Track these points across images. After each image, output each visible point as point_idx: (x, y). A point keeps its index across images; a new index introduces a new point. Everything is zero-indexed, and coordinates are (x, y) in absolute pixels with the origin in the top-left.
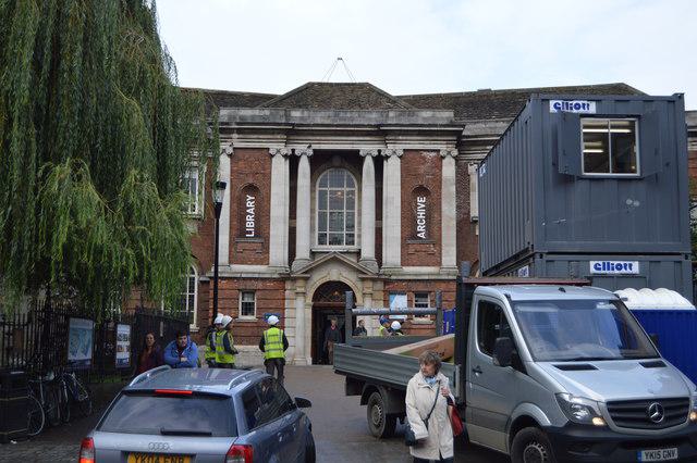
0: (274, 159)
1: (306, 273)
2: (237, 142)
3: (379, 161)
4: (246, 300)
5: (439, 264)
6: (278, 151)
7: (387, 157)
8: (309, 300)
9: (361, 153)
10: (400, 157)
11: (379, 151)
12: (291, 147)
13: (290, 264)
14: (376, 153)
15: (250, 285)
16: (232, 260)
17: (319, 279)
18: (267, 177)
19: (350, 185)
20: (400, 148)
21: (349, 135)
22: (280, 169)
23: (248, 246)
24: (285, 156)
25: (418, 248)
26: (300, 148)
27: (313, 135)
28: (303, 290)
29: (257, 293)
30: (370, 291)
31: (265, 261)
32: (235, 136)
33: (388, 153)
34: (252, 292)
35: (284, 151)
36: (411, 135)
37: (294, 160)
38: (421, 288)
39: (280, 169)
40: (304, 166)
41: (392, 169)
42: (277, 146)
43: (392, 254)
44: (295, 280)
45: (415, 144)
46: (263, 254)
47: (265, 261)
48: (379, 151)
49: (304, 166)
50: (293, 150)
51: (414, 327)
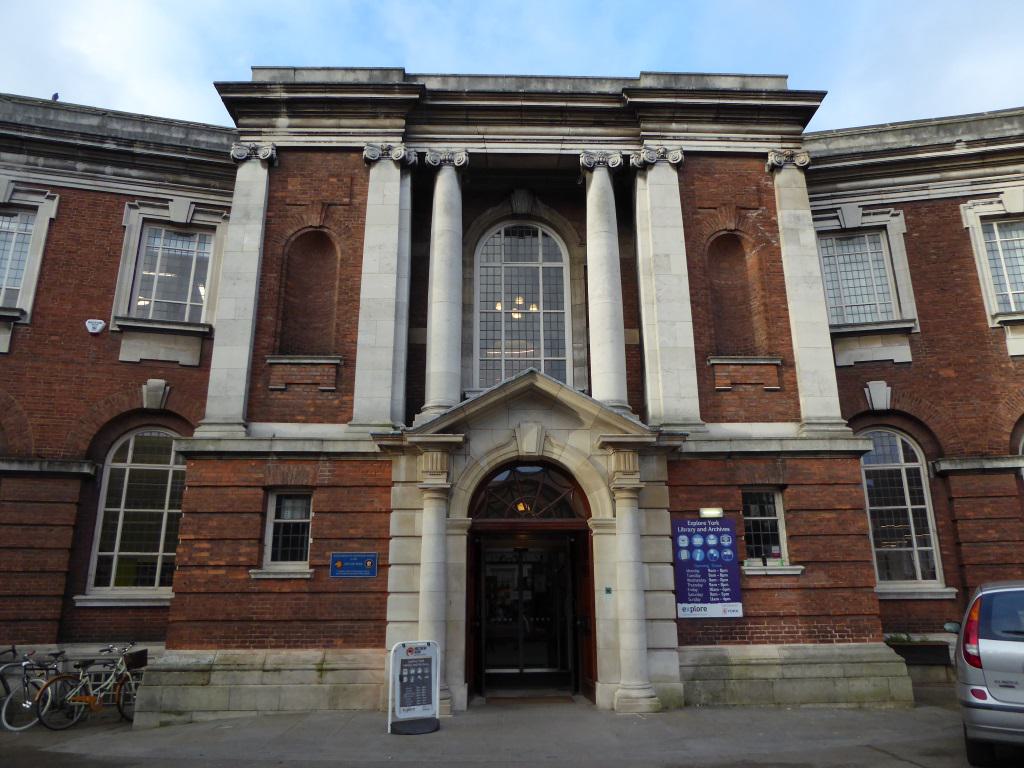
0: (374, 172)
1: (451, 429)
2: (283, 133)
3: (624, 180)
4: (288, 518)
5: (793, 415)
6: (386, 152)
7: (646, 166)
8: (460, 514)
9: (582, 160)
10: (677, 167)
11: (626, 158)
12: (423, 147)
13: (409, 421)
14: (616, 160)
15: (294, 474)
16: (257, 407)
17: (488, 448)
18: (356, 211)
19: (553, 254)
20: (676, 150)
21: (552, 124)
22: (385, 194)
23: (295, 374)
24: (403, 164)
25: (740, 374)
26: (435, 151)
27: (467, 123)
28: (441, 481)
29: (316, 496)
30: (634, 481)
31: (340, 412)
32: (283, 121)
33: (644, 156)
34: (302, 494)
35: (399, 150)
36: (699, 121)
37: (420, 177)
38: (760, 475)
39: (385, 194)
40: (446, 189)
41: (659, 199)
42: (381, 138)
43: (673, 390)
44: (414, 450)
45: (709, 139)
46: (336, 401)
47: (340, 412)
48: (626, 158)
49: (446, 189)
50: (422, 156)
51: (753, 584)
